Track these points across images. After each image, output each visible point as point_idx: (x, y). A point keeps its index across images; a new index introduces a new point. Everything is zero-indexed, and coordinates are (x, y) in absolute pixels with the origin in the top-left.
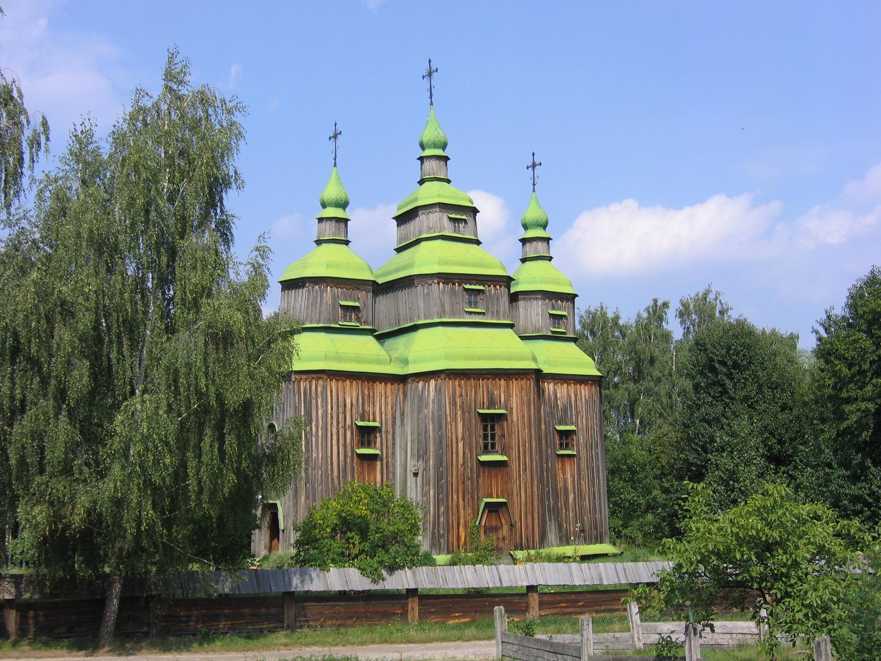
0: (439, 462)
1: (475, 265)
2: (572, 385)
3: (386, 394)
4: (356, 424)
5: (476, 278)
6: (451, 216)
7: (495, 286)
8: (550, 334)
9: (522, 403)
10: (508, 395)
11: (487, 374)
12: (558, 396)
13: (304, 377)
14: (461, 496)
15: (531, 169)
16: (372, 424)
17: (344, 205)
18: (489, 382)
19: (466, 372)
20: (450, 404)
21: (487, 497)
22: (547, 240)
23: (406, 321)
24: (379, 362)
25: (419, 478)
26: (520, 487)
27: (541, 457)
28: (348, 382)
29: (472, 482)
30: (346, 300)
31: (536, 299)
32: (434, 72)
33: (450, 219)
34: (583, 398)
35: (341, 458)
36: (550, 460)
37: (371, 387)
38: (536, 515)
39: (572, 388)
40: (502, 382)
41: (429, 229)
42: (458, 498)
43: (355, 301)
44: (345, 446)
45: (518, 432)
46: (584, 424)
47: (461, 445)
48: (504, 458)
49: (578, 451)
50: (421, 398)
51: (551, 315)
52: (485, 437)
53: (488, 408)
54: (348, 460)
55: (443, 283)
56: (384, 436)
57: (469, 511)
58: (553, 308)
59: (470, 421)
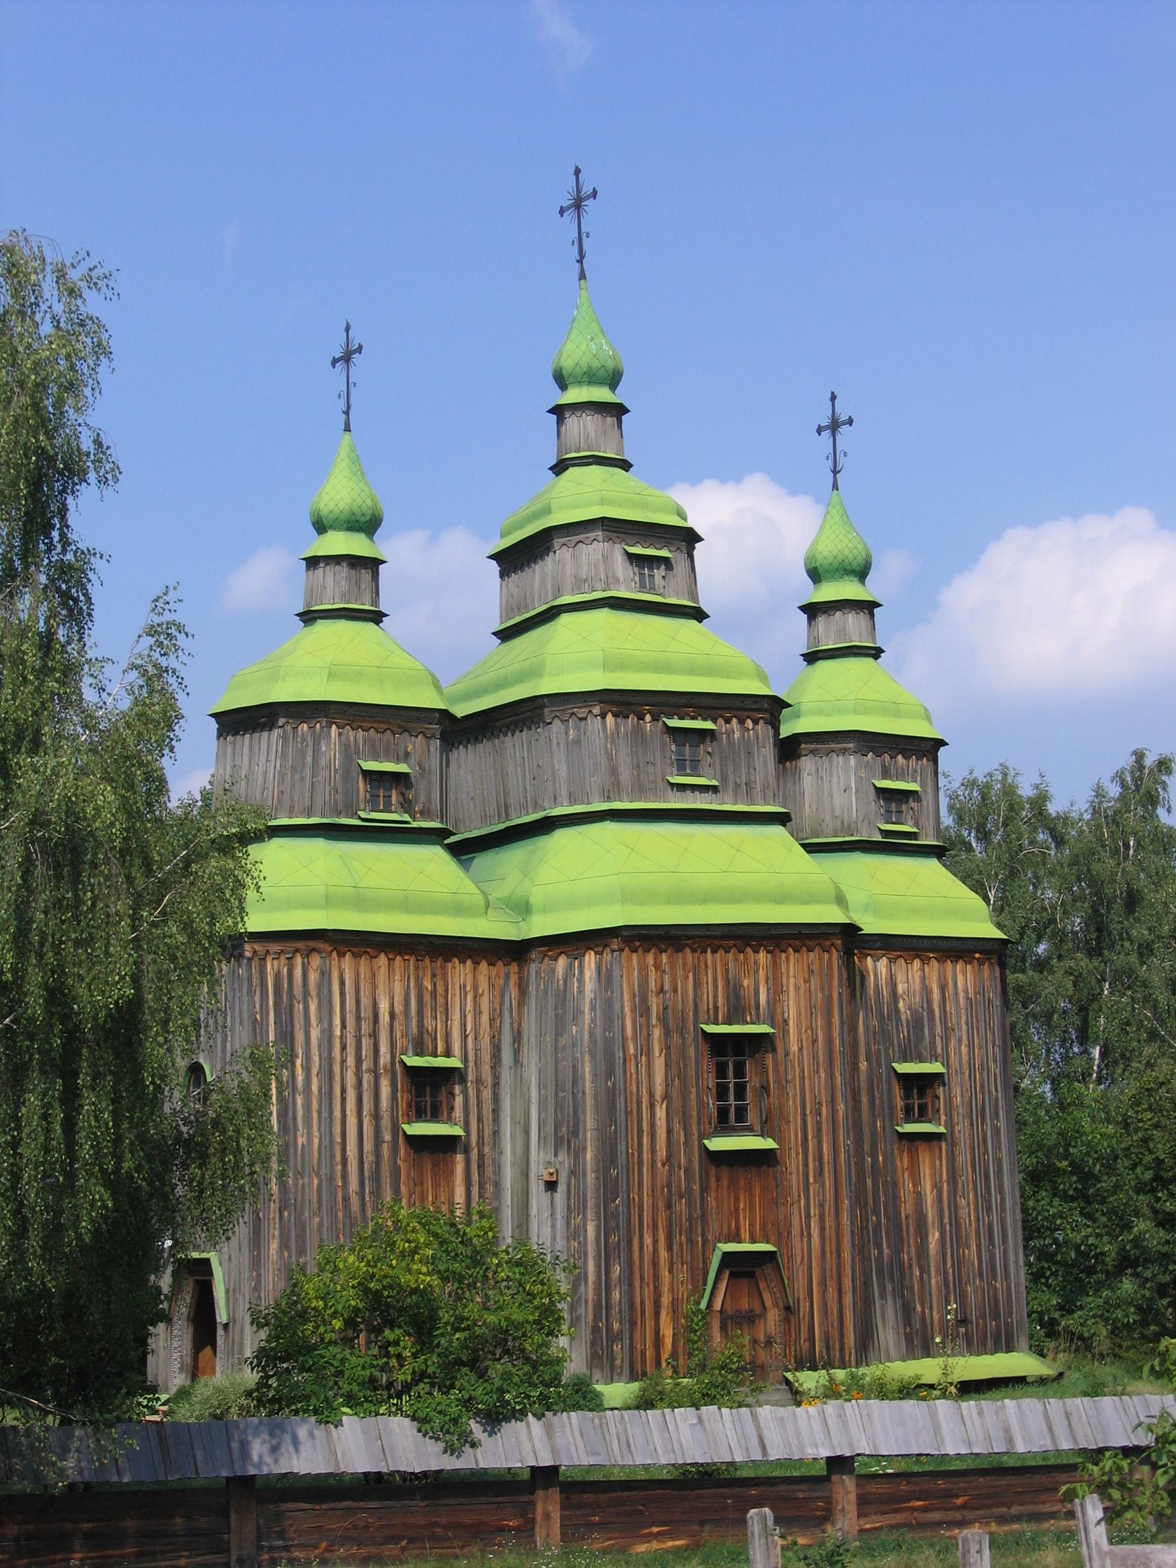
0: (608, 1155)
1: (691, 670)
2: (935, 963)
3: (475, 988)
4: (402, 1062)
5: (696, 700)
6: (632, 550)
7: (742, 722)
8: (878, 838)
9: (811, 1008)
10: (777, 990)
11: (723, 937)
12: (901, 989)
13: (275, 947)
14: (662, 1236)
15: (826, 434)
16: (441, 1062)
17: (368, 525)
18: (730, 956)
19: (673, 932)
20: (633, 1011)
21: (728, 1240)
22: (869, 607)
23: (524, 808)
24: (458, 909)
25: (560, 1195)
26: (808, 1216)
27: (859, 1141)
28: (382, 960)
29: (690, 1203)
30: (376, 757)
31: (844, 751)
32: (587, 198)
33: (632, 557)
34: (961, 995)
35: (368, 1146)
36: (881, 1146)
37: (439, 972)
38: (847, 1283)
39: (933, 970)
40: (763, 957)
41: (579, 583)
42: (655, 1242)
43: (398, 761)
44: (376, 1116)
45: (802, 1078)
46: (965, 1058)
47: (661, 1113)
48: (769, 1144)
49: (950, 1125)
50: (562, 998)
51: (882, 793)
52: (722, 1091)
53: (728, 1022)
54: (385, 1151)
55: (615, 715)
56: (472, 1092)
57: (683, 1274)
58: (886, 775)
59: (683, 1052)
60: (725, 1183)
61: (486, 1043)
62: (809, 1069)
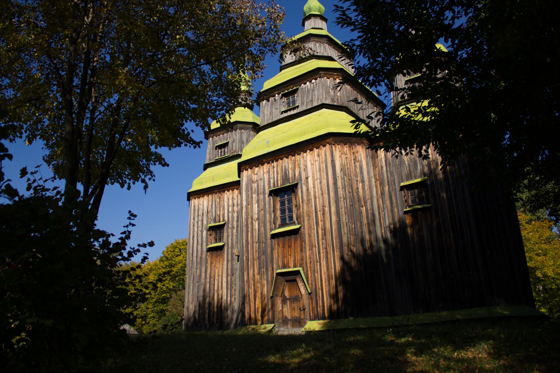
3: (233, 198)
42: (254, 271)
56: (230, 231)
60: (281, 246)
61: (235, 215)
62: (318, 194)
